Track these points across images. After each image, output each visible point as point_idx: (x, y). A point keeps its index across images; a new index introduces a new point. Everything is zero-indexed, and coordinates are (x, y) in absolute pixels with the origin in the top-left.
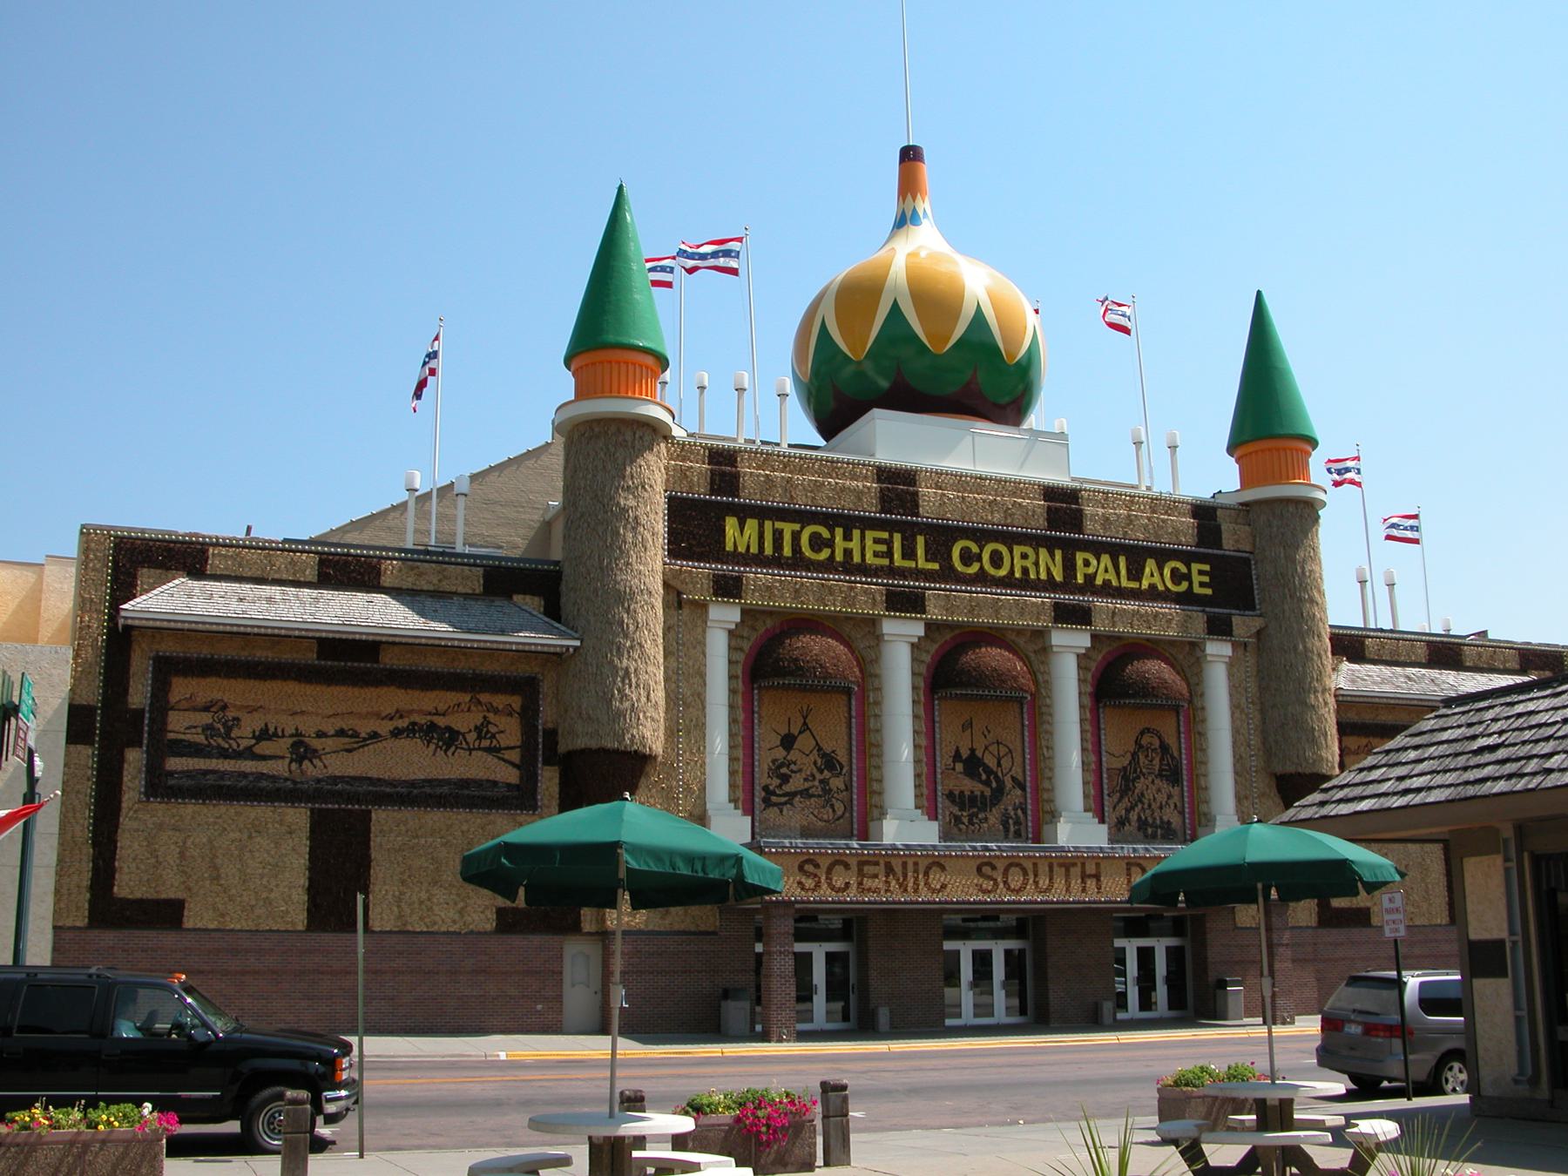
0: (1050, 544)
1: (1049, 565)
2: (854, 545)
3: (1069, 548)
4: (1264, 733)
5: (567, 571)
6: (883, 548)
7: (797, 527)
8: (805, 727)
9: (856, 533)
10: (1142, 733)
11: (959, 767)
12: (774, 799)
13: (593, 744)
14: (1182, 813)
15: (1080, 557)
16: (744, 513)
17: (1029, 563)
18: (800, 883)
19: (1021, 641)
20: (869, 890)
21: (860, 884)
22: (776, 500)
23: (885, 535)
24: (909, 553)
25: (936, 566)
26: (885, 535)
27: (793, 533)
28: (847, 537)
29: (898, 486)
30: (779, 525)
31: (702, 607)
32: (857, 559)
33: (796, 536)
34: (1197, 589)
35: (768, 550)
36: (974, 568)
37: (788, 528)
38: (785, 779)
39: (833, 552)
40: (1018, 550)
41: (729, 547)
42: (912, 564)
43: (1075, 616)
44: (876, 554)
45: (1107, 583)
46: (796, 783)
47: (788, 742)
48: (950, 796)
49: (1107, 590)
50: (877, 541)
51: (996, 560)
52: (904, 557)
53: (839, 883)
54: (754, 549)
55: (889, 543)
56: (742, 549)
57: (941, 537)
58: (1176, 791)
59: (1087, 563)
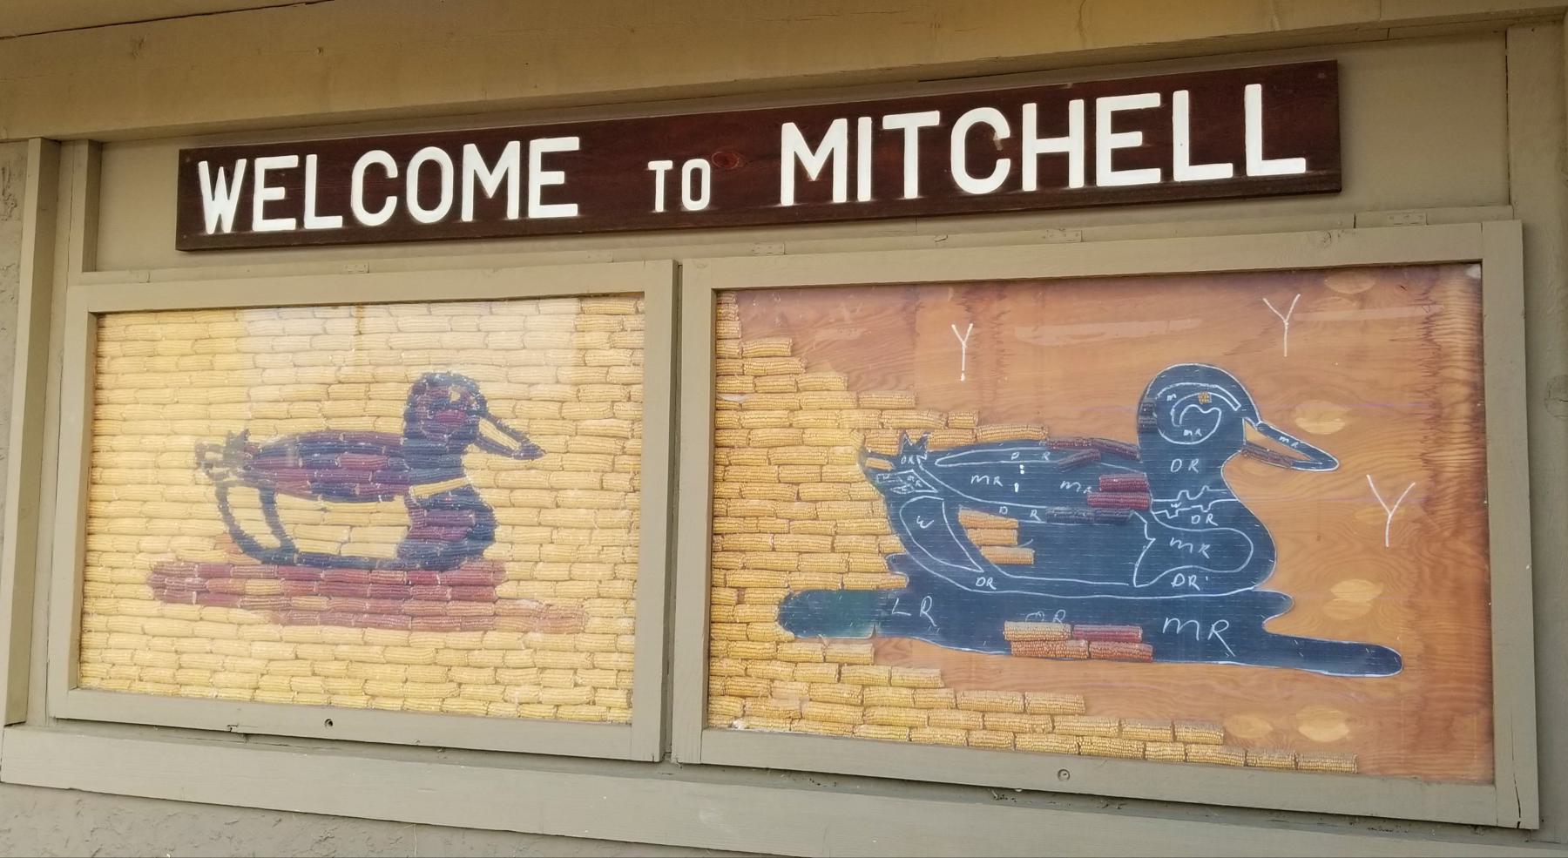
2: (1072, 145)
7: (932, 118)
9: (1076, 108)
23: (1152, 100)
24: (1216, 138)
25: (1296, 166)
26: (1152, 100)
27: (924, 133)
28: (1053, 125)
30: (891, 122)
32: (1076, 180)
33: (935, 142)
37: (911, 124)
39: (1016, 176)
44: (1123, 160)
55: (1156, 124)
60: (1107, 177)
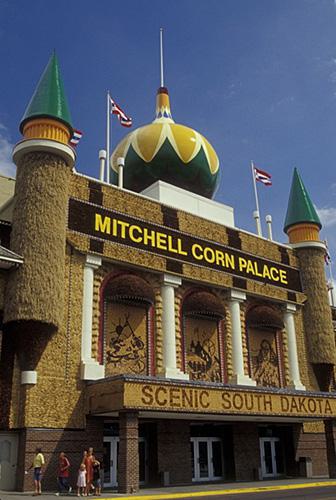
0: (230, 253)
1: (229, 261)
2: (152, 238)
3: (237, 256)
4: (308, 348)
5: (16, 225)
6: (164, 242)
8: (127, 324)
10: (264, 341)
11: (193, 350)
12: (112, 359)
13: (27, 317)
14: (279, 379)
15: (241, 259)
16: (104, 214)
17: (221, 259)
18: (143, 399)
19: (218, 294)
20: (175, 404)
21: (171, 401)
22: (120, 210)
23: (165, 236)
24: (175, 246)
25: (186, 254)
26: (165, 236)
29: (170, 215)
31: (82, 256)
32: (153, 245)
33: (127, 229)
34: (282, 281)
35: (115, 234)
36: (201, 257)
37: (124, 225)
38: (118, 349)
40: (217, 252)
41: (97, 229)
42: (175, 251)
43: (240, 284)
44: (161, 244)
45: (251, 272)
46: (122, 351)
47: (119, 330)
48: (190, 363)
49: (250, 275)
50: (161, 238)
51: (209, 254)
52: (173, 248)
53: (161, 401)
54: (108, 232)
55: (167, 239)
56: (103, 231)
57: (188, 241)
58: (276, 369)
59: (243, 263)
60: (159, 246)
